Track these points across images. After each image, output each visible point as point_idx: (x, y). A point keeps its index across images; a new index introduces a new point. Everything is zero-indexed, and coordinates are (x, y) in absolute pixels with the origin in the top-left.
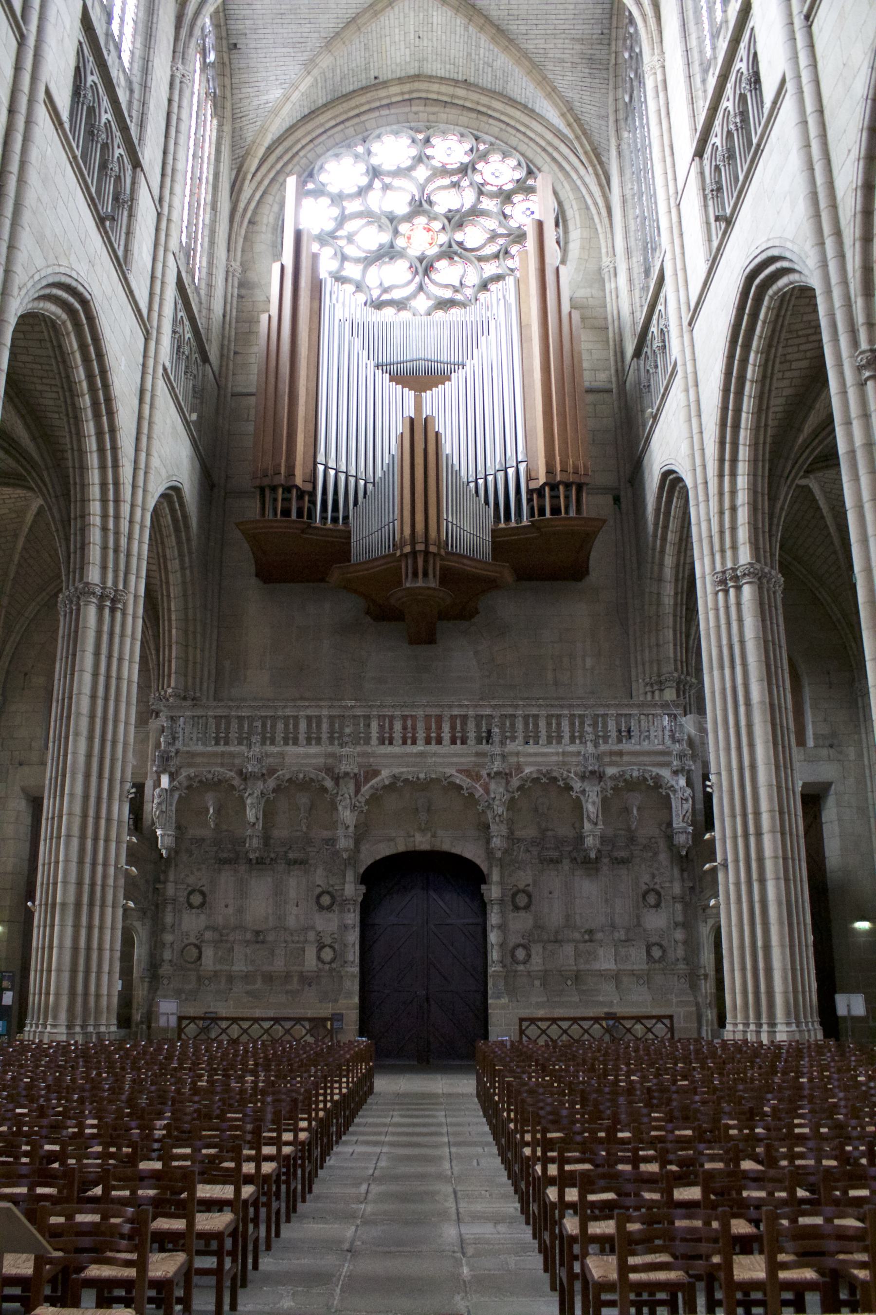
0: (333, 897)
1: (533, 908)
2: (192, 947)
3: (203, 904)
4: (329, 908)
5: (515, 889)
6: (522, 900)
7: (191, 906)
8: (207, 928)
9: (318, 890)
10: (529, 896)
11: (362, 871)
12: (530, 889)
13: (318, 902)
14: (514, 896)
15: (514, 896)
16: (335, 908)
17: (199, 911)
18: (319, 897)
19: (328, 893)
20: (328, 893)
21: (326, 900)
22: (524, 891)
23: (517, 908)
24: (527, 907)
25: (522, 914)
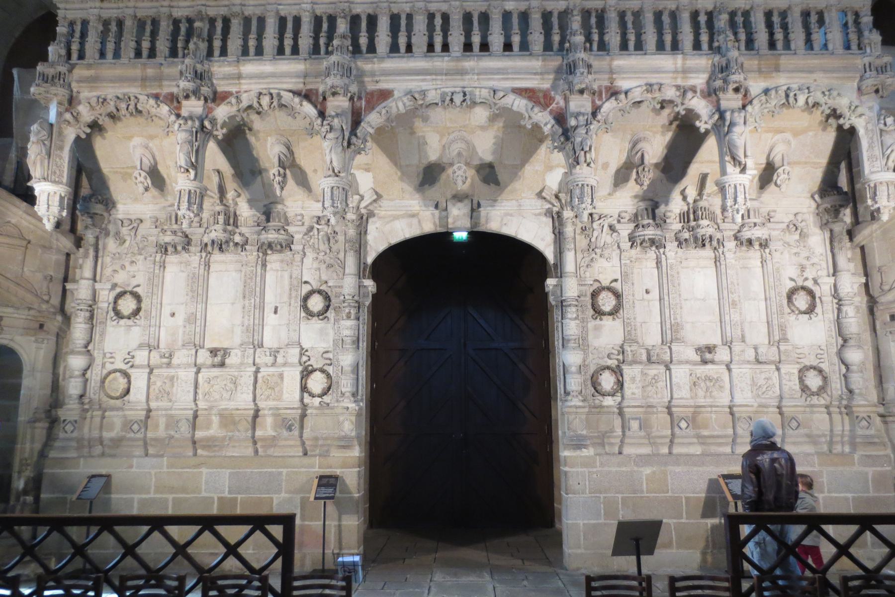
0: (327, 298)
1: (625, 313)
2: (118, 374)
3: (137, 311)
4: (322, 314)
5: (596, 285)
6: (607, 302)
7: (118, 315)
8: (140, 346)
9: (306, 289)
10: (618, 295)
11: (370, 260)
12: (617, 286)
13: (305, 307)
14: (595, 295)
15: (595, 295)
16: (331, 314)
17: (130, 322)
18: (306, 299)
19: (320, 292)
20: (320, 292)
21: (316, 303)
22: (609, 289)
23: (598, 313)
24: (614, 313)
25: (607, 321)
